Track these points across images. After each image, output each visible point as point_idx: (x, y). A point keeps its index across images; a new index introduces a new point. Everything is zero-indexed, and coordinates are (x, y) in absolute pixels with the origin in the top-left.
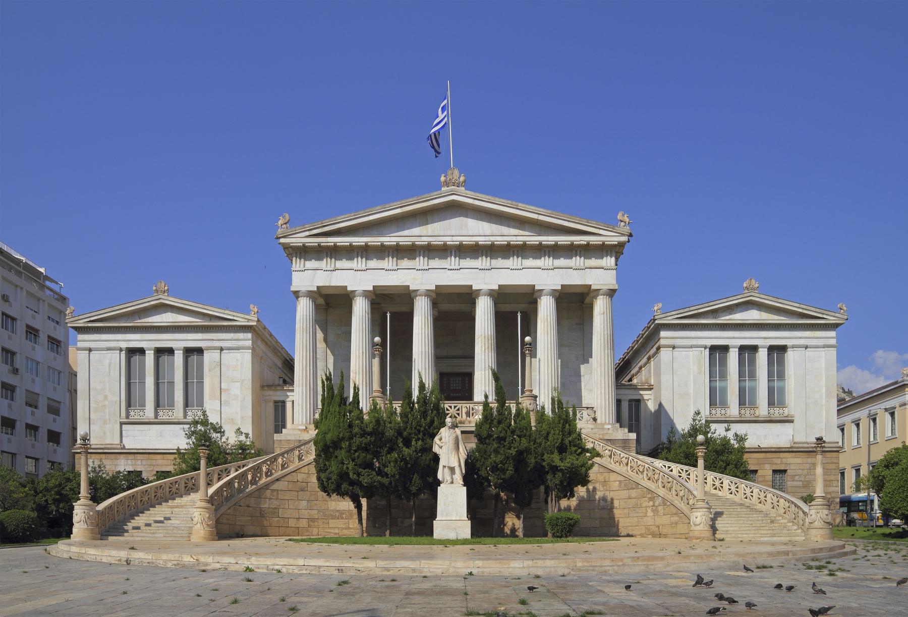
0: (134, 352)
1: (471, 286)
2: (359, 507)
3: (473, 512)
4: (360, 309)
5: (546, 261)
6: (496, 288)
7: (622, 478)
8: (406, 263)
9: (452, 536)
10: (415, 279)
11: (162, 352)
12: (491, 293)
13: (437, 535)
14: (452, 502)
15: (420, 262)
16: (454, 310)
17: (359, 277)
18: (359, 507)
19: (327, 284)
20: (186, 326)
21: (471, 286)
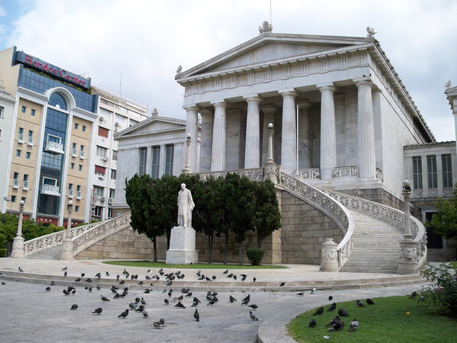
0: (143, 150)
1: (277, 91)
2: (154, 241)
3: (198, 245)
4: (220, 114)
5: (326, 67)
6: (292, 90)
7: (329, 221)
8: (242, 82)
9: (175, 261)
10: (246, 91)
11: (156, 148)
12: (291, 94)
13: (167, 261)
14: (184, 238)
15: (250, 79)
16: (271, 107)
17: (216, 95)
18: (154, 241)
19: (200, 102)
20: (158, 133)
21: (277, 91)
